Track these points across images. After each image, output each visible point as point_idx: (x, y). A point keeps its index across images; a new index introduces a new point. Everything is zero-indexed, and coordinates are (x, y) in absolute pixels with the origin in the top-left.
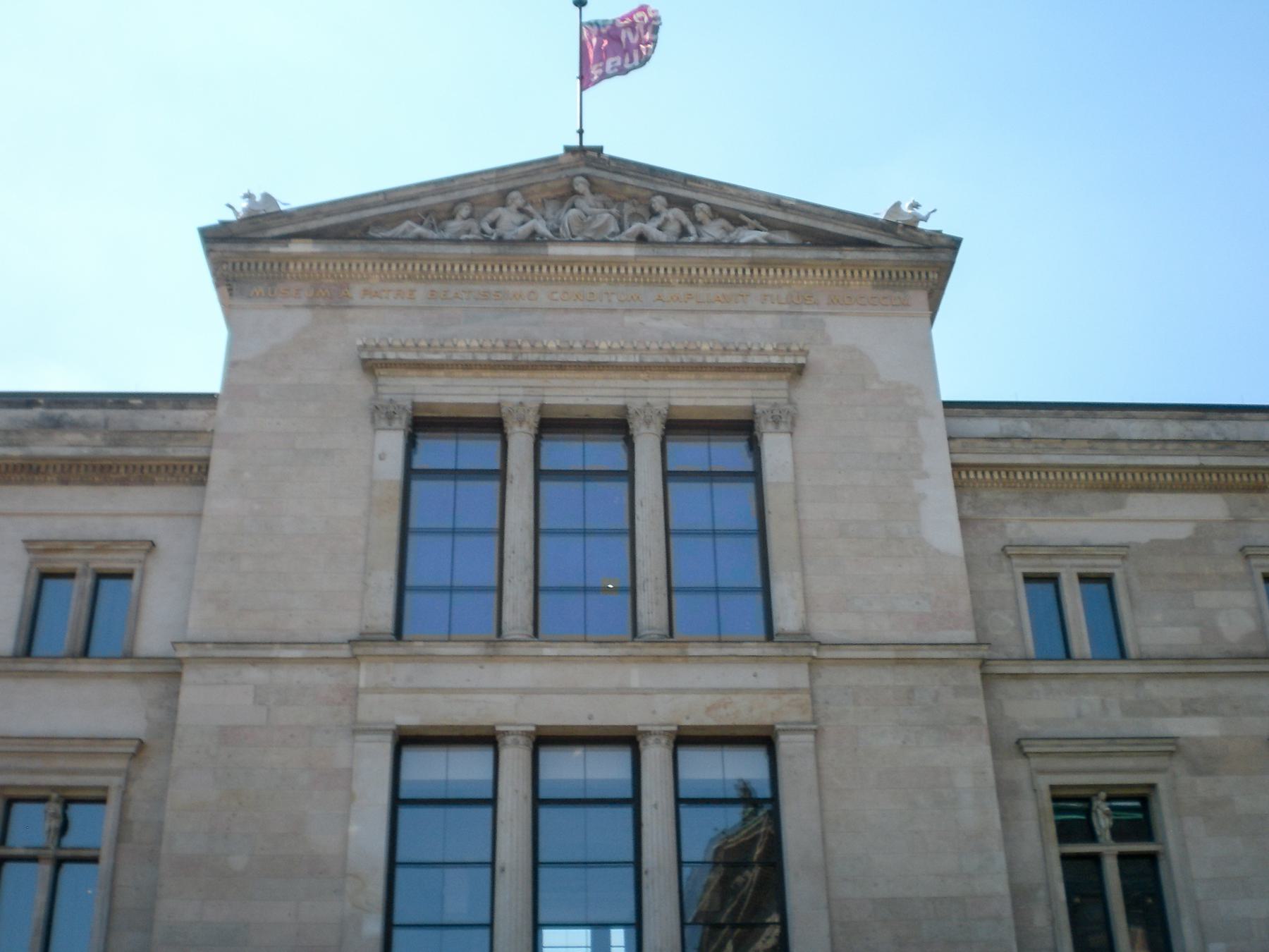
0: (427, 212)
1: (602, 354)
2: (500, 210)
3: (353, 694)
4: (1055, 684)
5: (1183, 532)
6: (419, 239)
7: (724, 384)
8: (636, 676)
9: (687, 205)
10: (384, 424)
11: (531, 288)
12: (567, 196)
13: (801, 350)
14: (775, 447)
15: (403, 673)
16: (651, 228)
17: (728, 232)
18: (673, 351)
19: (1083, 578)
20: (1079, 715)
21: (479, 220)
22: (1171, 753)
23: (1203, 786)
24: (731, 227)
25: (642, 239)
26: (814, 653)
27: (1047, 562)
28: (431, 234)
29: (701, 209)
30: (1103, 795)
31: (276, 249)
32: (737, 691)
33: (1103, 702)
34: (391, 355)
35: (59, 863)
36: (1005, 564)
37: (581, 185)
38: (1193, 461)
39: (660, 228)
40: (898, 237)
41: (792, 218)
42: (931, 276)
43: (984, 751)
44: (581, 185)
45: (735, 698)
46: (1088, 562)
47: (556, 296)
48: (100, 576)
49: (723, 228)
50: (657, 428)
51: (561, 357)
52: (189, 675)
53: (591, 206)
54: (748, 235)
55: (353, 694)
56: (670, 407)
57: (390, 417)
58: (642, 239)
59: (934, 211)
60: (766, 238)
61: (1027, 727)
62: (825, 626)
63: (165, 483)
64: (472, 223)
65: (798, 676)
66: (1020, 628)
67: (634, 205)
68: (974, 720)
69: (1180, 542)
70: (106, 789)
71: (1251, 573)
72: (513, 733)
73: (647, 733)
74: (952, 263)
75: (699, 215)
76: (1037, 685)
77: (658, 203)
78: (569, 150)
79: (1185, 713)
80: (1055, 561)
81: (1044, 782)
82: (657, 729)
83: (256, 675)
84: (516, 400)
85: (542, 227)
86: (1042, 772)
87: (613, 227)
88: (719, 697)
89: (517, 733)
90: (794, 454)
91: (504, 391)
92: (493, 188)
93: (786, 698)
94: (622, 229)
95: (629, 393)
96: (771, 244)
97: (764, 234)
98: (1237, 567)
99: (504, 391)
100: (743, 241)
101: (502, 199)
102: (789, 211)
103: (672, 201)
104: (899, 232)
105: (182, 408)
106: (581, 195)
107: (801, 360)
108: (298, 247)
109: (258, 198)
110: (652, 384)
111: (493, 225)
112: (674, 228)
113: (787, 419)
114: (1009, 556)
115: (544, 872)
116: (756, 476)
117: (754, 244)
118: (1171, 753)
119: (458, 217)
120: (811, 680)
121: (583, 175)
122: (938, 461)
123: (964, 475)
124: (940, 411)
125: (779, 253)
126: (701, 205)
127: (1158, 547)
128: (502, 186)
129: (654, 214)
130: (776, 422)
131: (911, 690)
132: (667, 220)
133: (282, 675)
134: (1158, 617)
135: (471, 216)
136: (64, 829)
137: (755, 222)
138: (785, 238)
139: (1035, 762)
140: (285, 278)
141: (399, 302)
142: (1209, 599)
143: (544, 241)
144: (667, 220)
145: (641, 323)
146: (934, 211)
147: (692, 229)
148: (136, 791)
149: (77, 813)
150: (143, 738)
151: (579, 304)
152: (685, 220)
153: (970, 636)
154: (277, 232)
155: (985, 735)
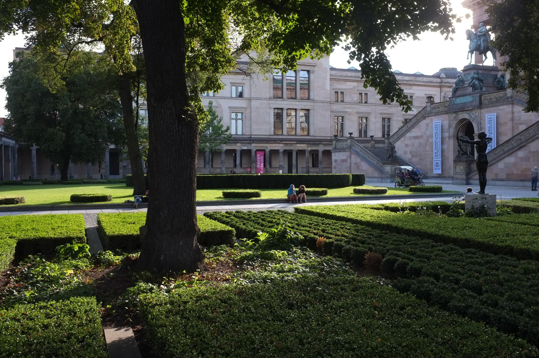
5: (352, 87)
8: (297, 103)
14: (312, 76)
52: (252, 101)
65: (312, 104)
83: (259, 101)
98: (356, 92)
113: (313, 72)
122: (328, 78)
127: (349, 89)
133: (262, 101)
142: (353, 95)
153: (329, 100)
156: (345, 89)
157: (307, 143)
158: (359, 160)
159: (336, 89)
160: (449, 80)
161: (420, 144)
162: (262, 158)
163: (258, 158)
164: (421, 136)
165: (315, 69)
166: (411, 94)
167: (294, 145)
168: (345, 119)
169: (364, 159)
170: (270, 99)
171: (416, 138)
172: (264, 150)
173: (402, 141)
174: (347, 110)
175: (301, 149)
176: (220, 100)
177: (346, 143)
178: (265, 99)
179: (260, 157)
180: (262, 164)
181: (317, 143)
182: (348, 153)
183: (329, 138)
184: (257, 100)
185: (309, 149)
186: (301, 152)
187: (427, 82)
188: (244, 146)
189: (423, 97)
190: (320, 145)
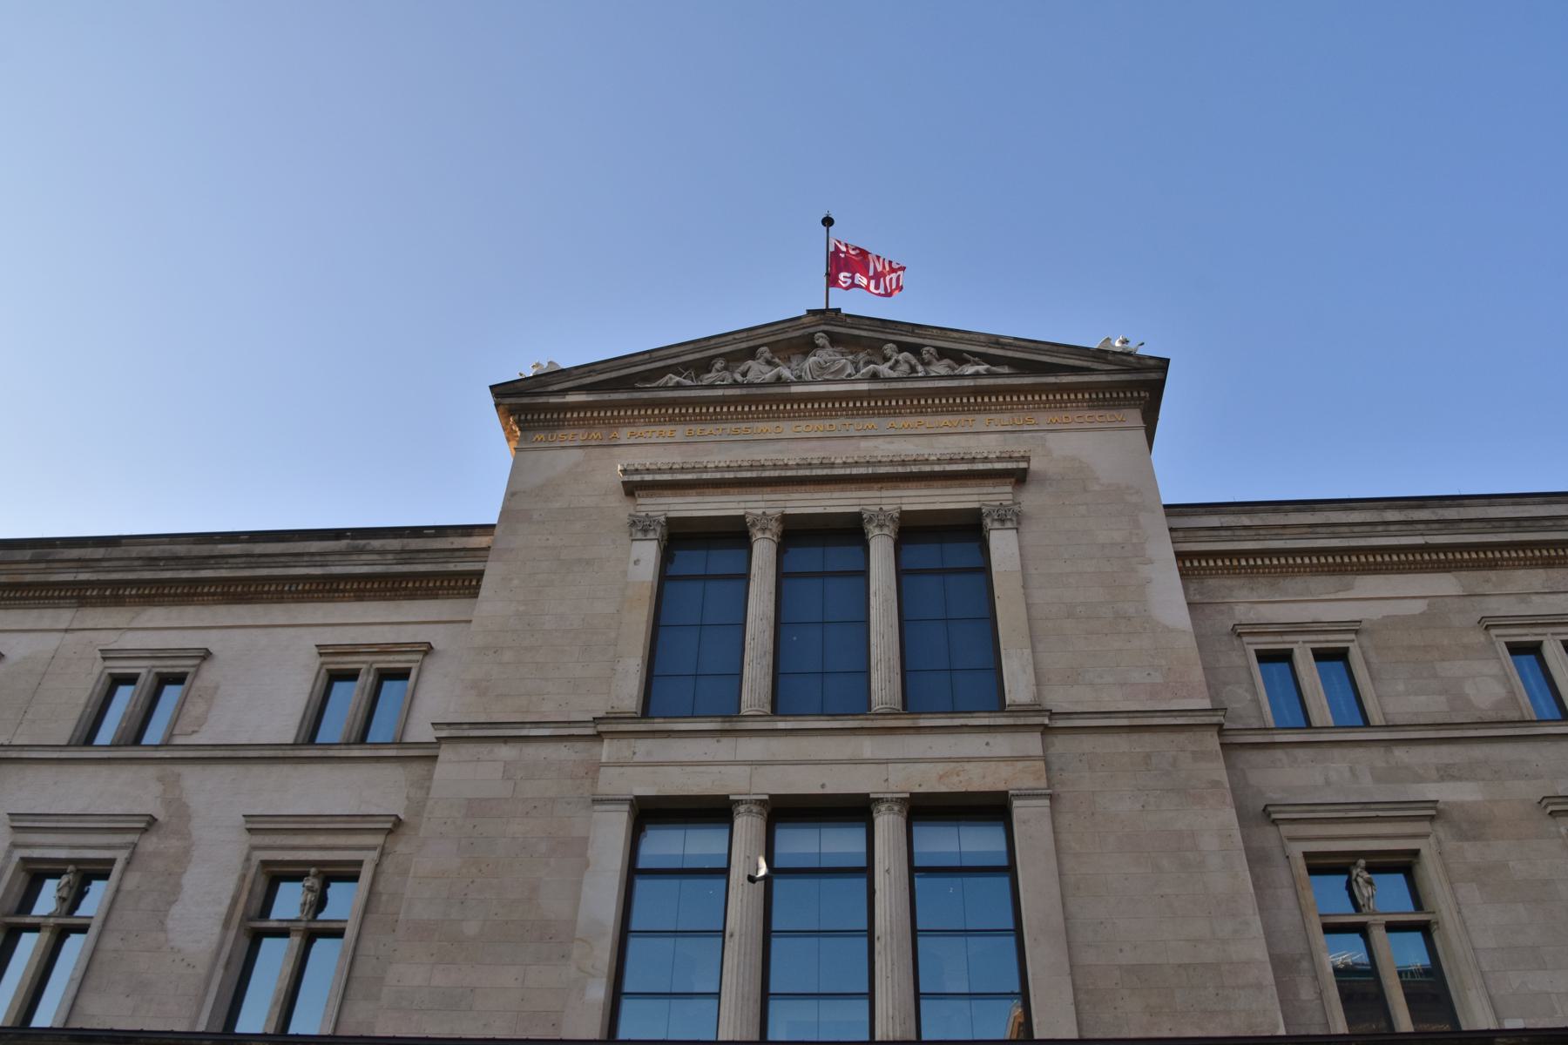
0: (687, 366)
1: (838, 468)
2: (750, 362)
4: (1300, 753)
5: (1418, 607)
6: (678, 386)
7: (952, 491)
8: (868, 747)
10: (640, 535)
11: (776, 424)
12: (807, 346)
13: (1023, 457)
14: (1002, 545)
16: (884, 369)
17: (953, 369)
18: (903, 463)
19: (1321, 655)
20: (1328, 783)
21: (732, 372)
22: (1432, 818)
23: (1472, 852)
24: (956, 366)
25: (875, 377)
26: (1046, 721)
27: (1279, 639)
28: (688, 382)
29: (928, 351)
30: (1362, 862)
31: (553, 400)
32: (969, 760)
33: (1351, 769)
34: (648, 477)
35: (311, 937)
36: (1236, 642)
37: (821, 340)
38: (1419, 540)
39: (891, 368)
40: (1110, 363)
41: (1010, 354)
42: (1142, 394)
43: (1229, 816)
44: (821, 340)
45: (967, 766)
46: (1322, 637)
47: (799, 429)
48: (385, 675)
49: (949, 366)
50: (890, 530)
51: (801, 473)
53: (830, 356)
54: (969, 370)
56: (903, 514)
57: (645, 531)
58: (875, 377)
59: (1142, 344)
60: (987, 370)
61: (1275, 796)
62: (1058, 699)
63: (448, 597)
64: (727, 374)
65: (1032, 743)
66: (1256, 701)
67: (868, 354)
68: (1216, 784)
69: (1414, 616)
70: (360, 863)
71: (1493, 643)
72: (746, 802)
73: (879, 801)
74: (1162, 382)
75: (926, 356)
76: (1279, 754)
77: (889, 349)
78: (811, 312)
79: (1442, 779)
80: (1287, 638)
81: (1297, 849)
82: (889, 796)
83: (506, 752)
84: (760, 512)
85: (786, 373)
86: (1292, 839)
87: (850, 370)
88: (953, 765)
89: (751, 802)
90: (1021, 548)
91: (749, 505)
92: (744, 345)
93: (1020, 765)
94: (857, 371)
95: (863, 502)
96: (990, 374)
97: (986, 366)
98: (1479, 638)
99: (749, 505)
100: (967, 373)
101: (751, 353)
102: (1008, 347)
103: (902, 347)
104: (1110, 358)
105: (470, 535)
106: (823, 347)
107: (1023, 465)
108: (572, 398)
109: (546, 365)
110: (885, 493)
111: (744, 374)
112: (904, 368)
114: (1239, 635)
115: (776, 943)
116: (985, 570)
117: (977, 375)
118: (1432, 818)
119: (714, 369)
120: (1045, 748)
121: (823, 332)
122: (1163, 552)
123: (1188, 564)
124: (1162, 512)
125: (1000, 381)
126: (927, 348)
127: (1391, 622)
128: (751, 344)
129: (886, 359)
130: (1002, 521)
131: (1148, 756)
132: (897, 362)
133: (532, 751)
134: (1401, 687)
135: (726, 368)
136: (321, 903)
137: (977, 359)
138: (1006, 370)
139: (1286, 830)
140: (564, 425)
141: (661, 440)
143: (788, 383)
144: (897, 362)
145: (876, 447)
146: (1142, 344)
147: (920, 368)
148: (388, 864)
149: (336, 891)
150: (402, 817)
151: (819, 434)
152: (914, 361)
153: (1206, 704)
154: (556, 388)
155: (1229, 799)
156: (1355, 628)
159: (1257, 630)
165: (1030, 499)
170: (602, 728)
184: (483, 750)
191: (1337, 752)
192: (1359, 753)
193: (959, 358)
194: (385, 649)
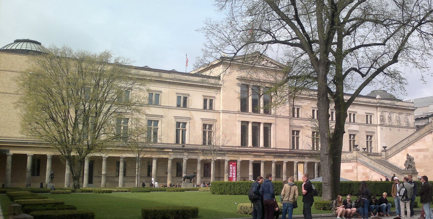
3: (237, 117)
8: (261, 117)
9: (268, 61)
15: (242, 115)
55: (237, 117)
65: (274, 118)
68: (288, 124)
76: (292, 119)
83: (228, 114)
103: (266, 60)
129: (264, 60)
138: (276, 66)
157: (274, 154)
158: (368, 170)
160: (384, 101)
161: (425, 157)
162: (234, 168)
163: (231, 168)
164: (426, 149)
166: (354, 112)
167: (262, 157)
168: (300, 133)
169: (374, 169)
171: (420, 150)
172: (236, 161)
173: (403, 154)
174: (303, 125)
175: (268, 160)
176: (193, 112)
177: (350, 155)
178: (234, 113)
179: (232, 167)
180: (234, 174)
181: (282, 155)
182: (354, 164)
183: (289, 151)
185: (276, 160)
186: (268, 164)
187: (366, 102)
188: (219, 156)
189: (364, 116)
190: (285, 157)
191: (296, 120)
192: (298, 120)
193: (272, 63)
194: (210, 97)
